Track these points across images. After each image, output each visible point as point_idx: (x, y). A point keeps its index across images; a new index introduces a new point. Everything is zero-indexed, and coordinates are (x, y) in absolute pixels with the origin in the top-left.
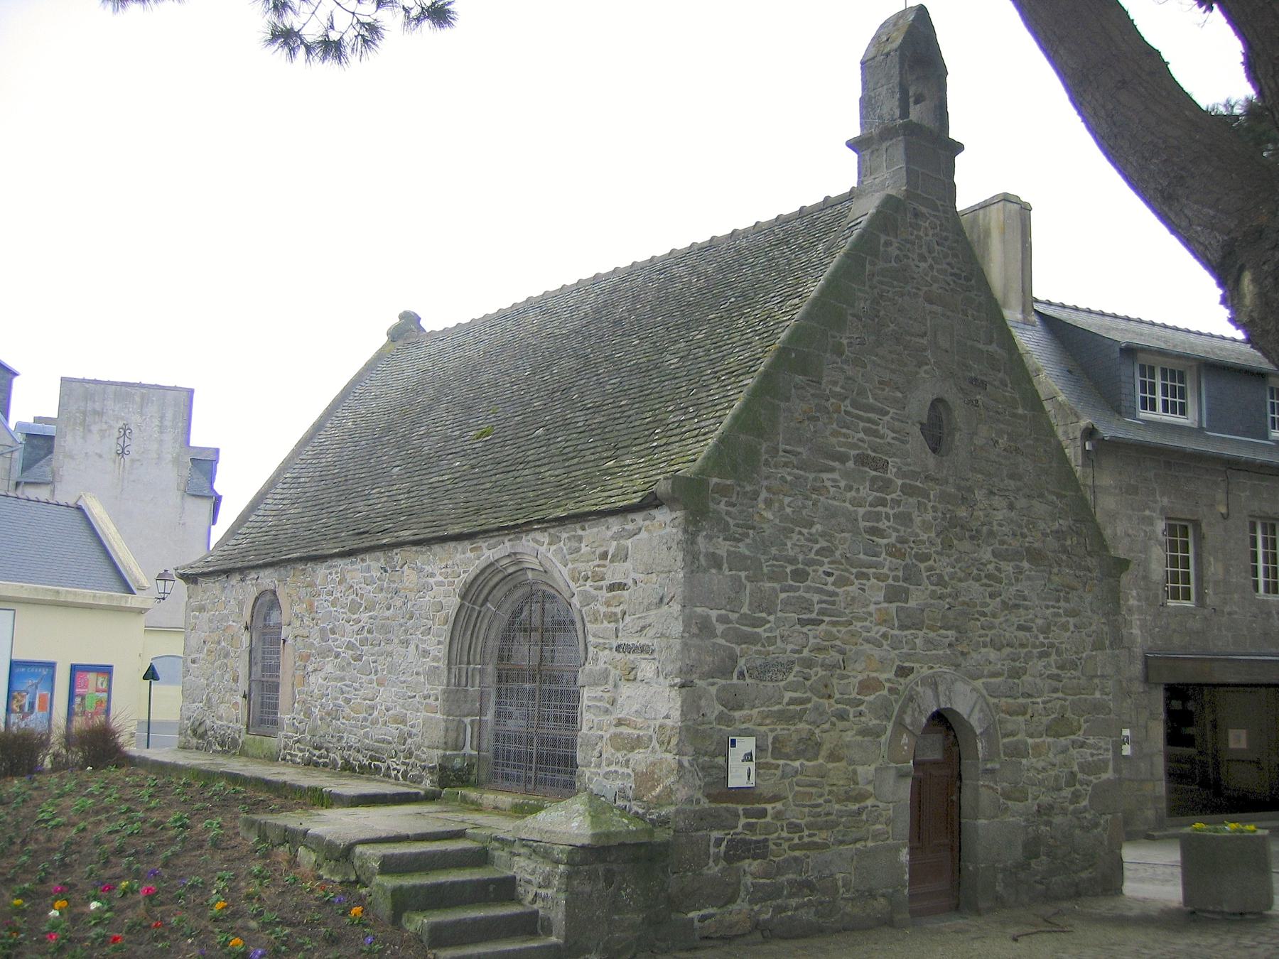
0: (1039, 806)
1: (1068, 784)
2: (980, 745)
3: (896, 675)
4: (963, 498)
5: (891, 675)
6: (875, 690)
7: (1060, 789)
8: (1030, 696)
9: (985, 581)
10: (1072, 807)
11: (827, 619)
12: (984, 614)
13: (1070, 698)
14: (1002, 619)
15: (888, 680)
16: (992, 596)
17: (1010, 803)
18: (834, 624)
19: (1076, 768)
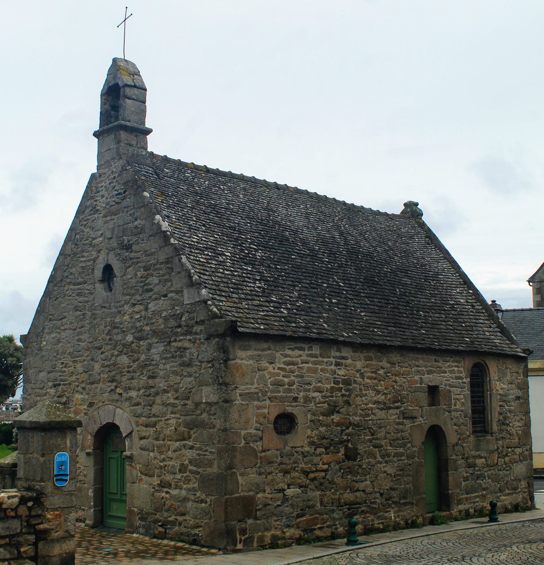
0: (161, 482)
1: (180, 471)
2: (127, 443)
3: (88, 406)
4: (120, 312)
5: (85, 407)
6: (79, 413)
7: (175, 474)
8: (157, 416)
9: (130, 354)
10: (185, 486)
11: (62, 383)
12: (128, 372)
13: (183, 418)
14: (139, 374)
15: (84, 409)
16: (134, 361)
17: (143, 477)
18: (64, 385)
19: (186, 462)
